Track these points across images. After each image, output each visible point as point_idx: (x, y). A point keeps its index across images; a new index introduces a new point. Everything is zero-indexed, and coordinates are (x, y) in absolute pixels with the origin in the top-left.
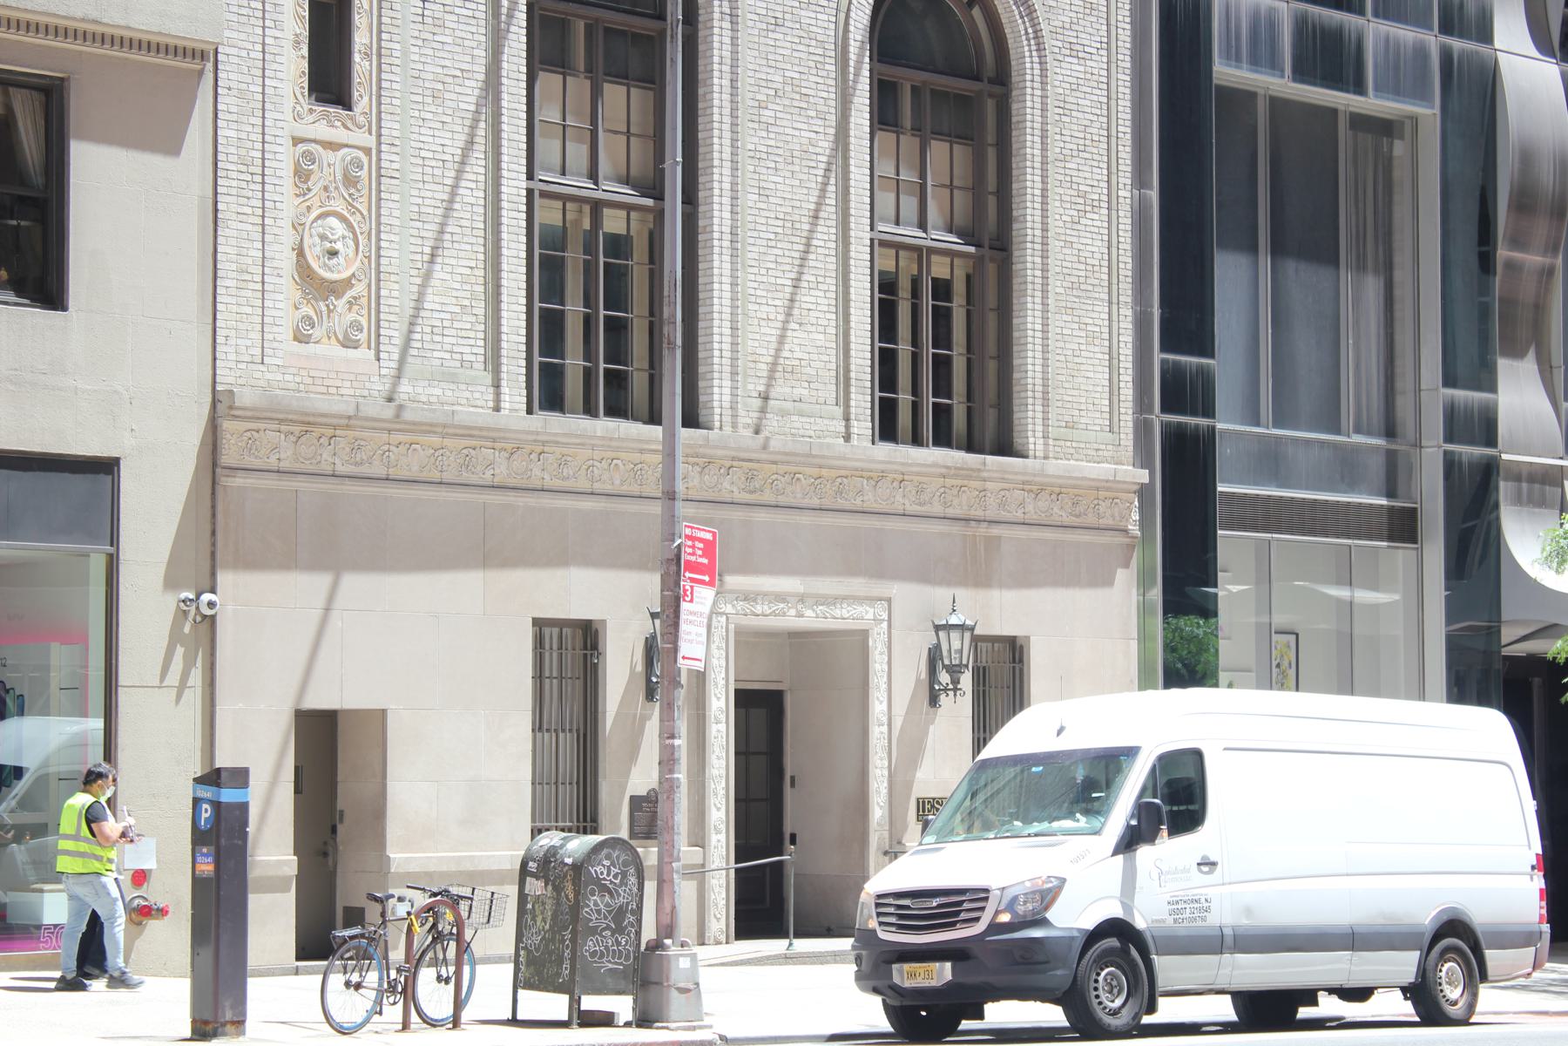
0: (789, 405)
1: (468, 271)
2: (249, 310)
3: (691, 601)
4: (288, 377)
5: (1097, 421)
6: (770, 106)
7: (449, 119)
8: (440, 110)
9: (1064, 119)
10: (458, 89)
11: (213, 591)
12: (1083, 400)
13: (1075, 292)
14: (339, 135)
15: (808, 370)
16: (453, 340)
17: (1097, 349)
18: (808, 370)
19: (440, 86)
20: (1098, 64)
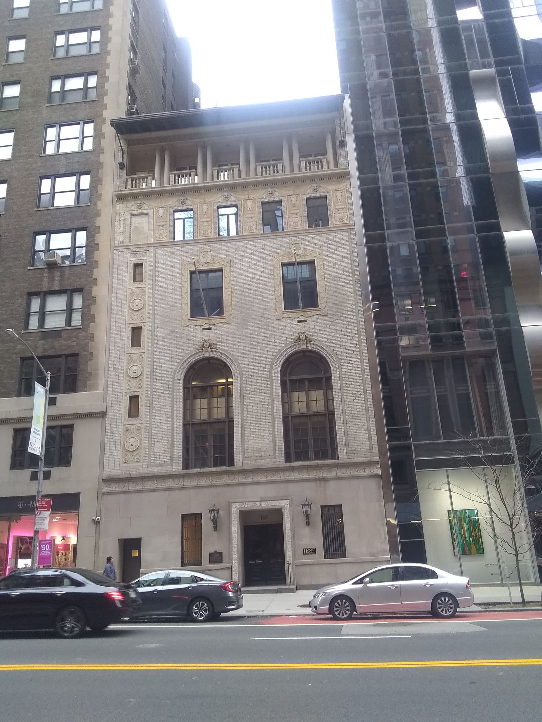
0: (258, 458)
1: (167, 443)
2: (112, 460)
3: (40, 515)
4: (120, 472)
5: (365, 448)
6: (250, 394)
7: (162, 414)
8: (160, 413)
9: (346, 378)
10: (164, 408)
11: (100, 517)
12: (359, 443)
13: (353, 417)
14: (135, 422)
15: (264, 449)
16: (162, 458)
17: (363, 430)
18: (264, 449)
19: (160, 408)
20: (358, 364)
